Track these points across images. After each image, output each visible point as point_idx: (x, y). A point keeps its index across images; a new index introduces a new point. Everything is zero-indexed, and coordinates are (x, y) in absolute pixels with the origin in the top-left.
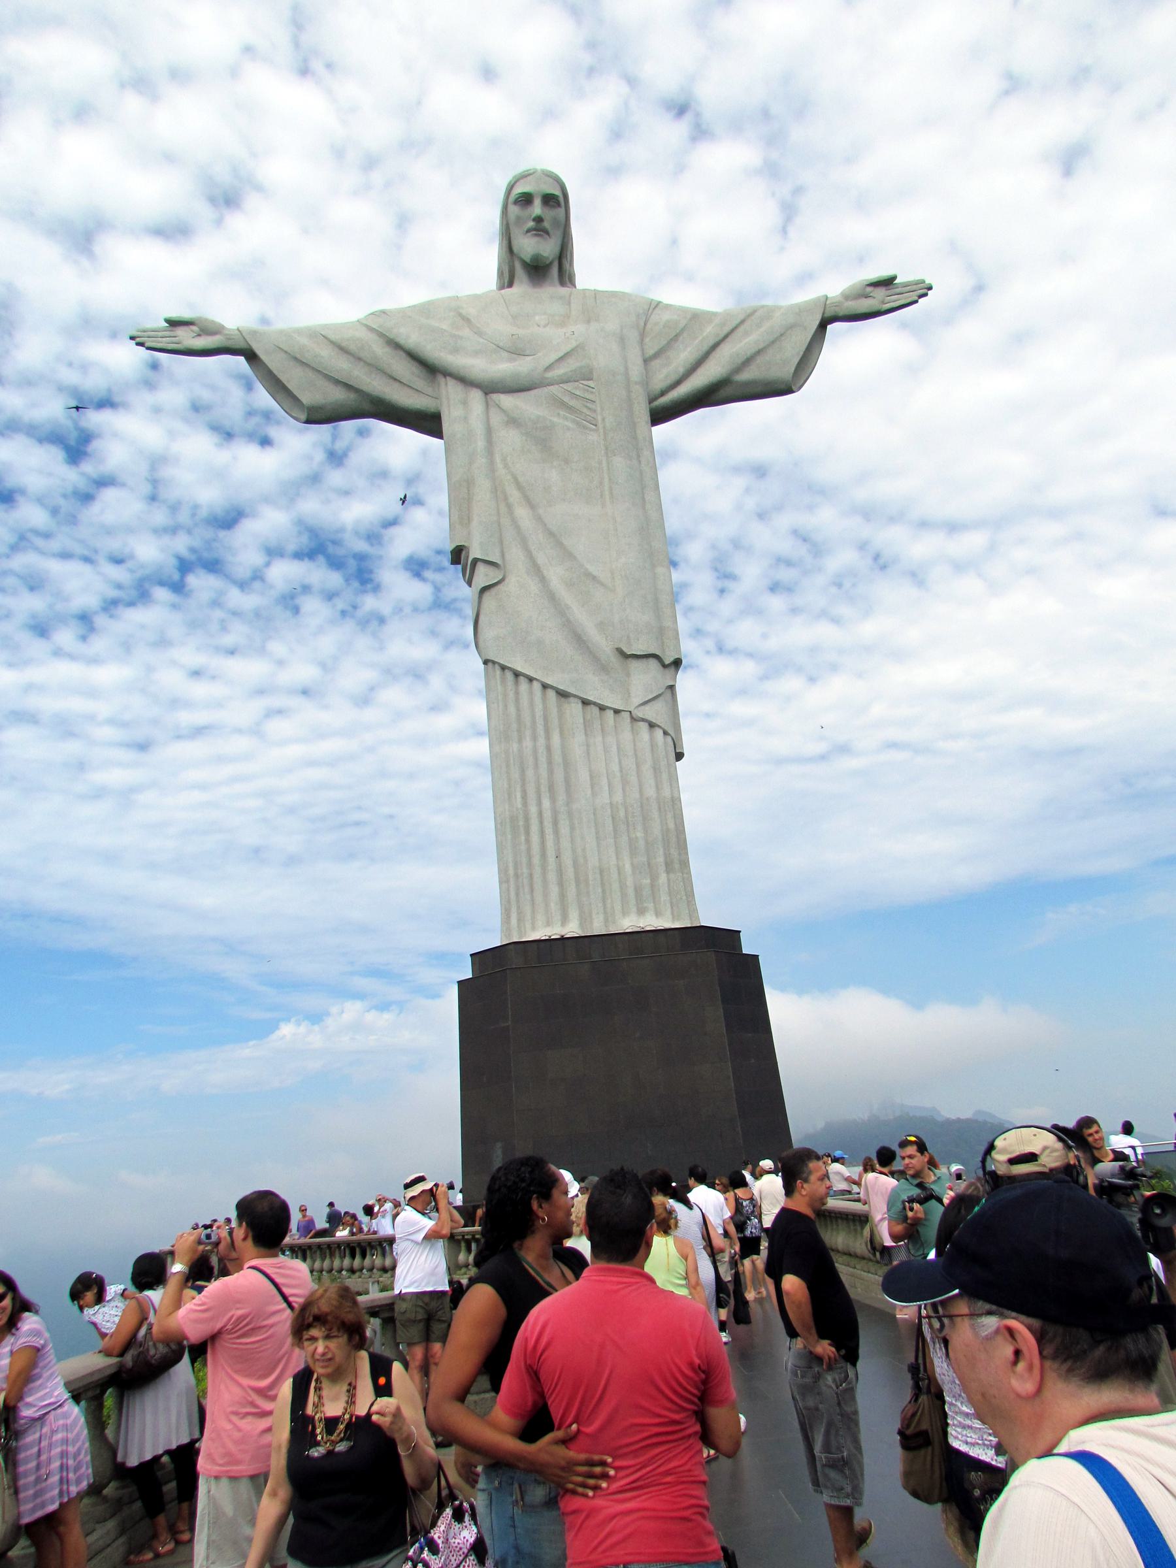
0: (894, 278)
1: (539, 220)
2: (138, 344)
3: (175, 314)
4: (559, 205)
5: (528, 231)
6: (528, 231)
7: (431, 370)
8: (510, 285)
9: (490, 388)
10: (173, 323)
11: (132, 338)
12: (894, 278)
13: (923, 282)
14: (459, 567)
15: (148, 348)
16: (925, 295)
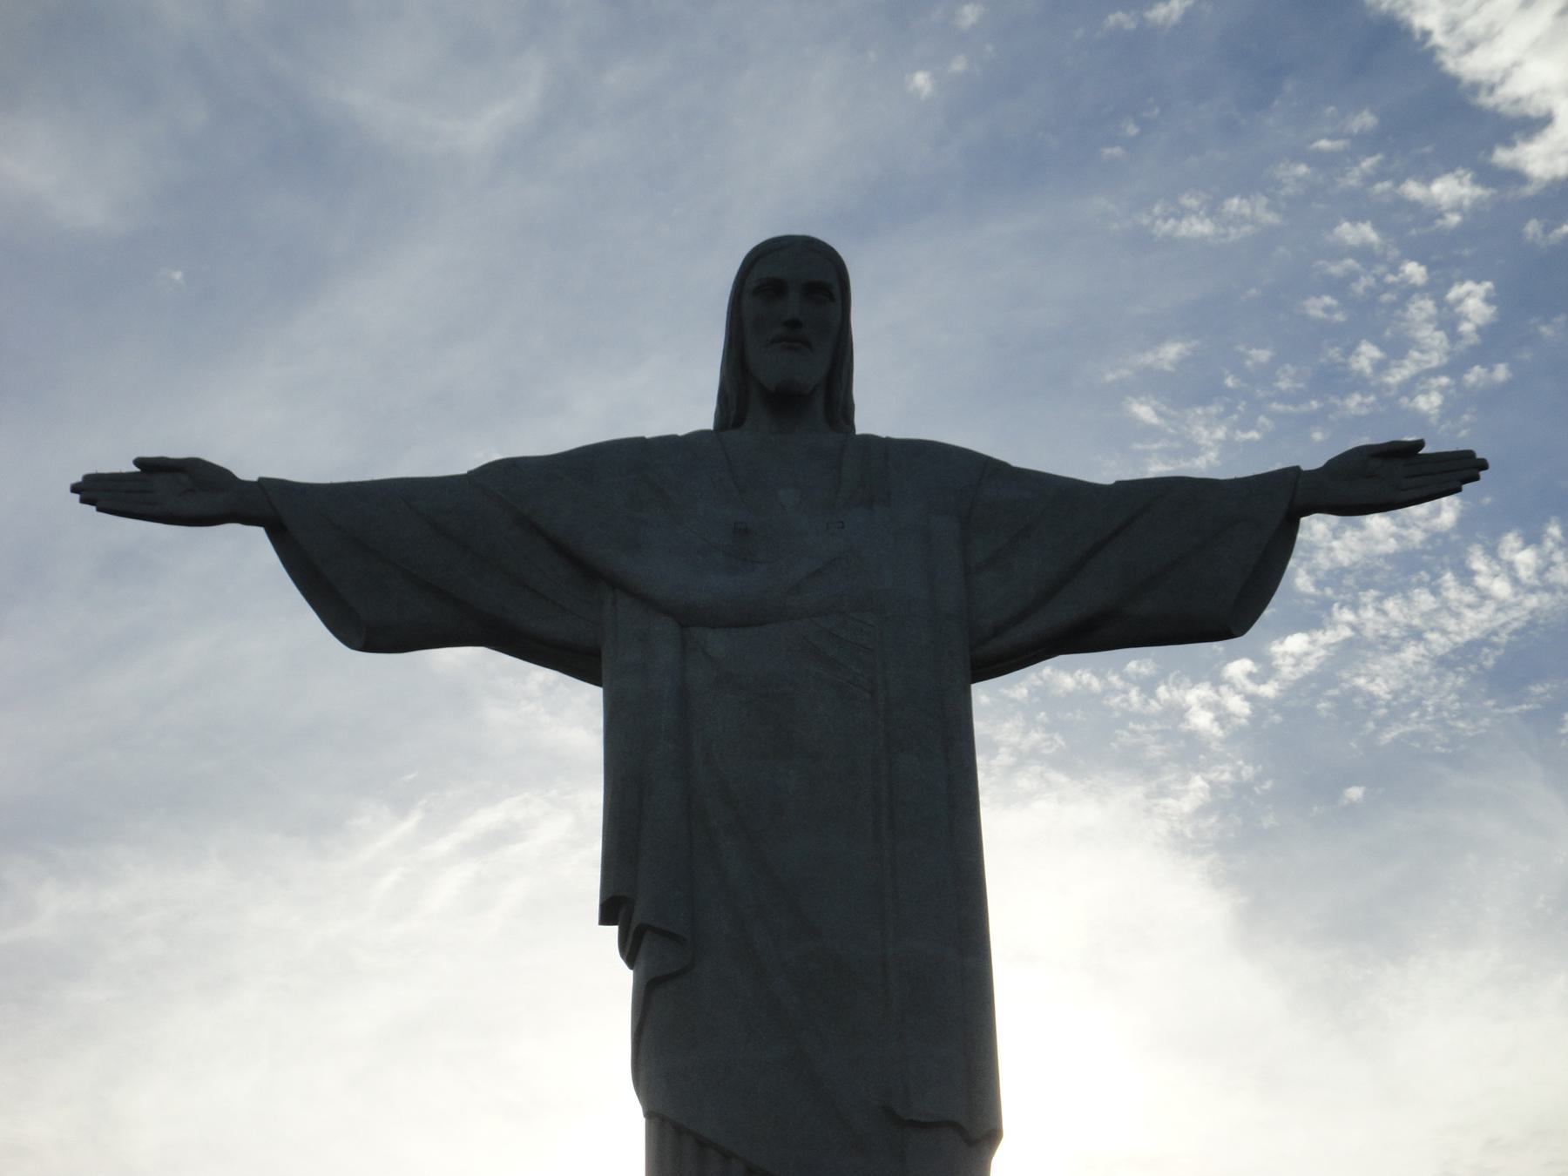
0: (1420, 444)
1: (795, 324)
2: (83, 501)
3: (152, 452)
4: (831, 297)
5: (773, 342)
6: (773, 342)
7: (591, 574)
8: (738, 422)
9: (688, 618)
10: (150, 467)
11: (75, 489)
12: (1420, 444)
13: (1469, 455)
14: (615, 929)
15: (99, 510)
16: (1477, 478)
